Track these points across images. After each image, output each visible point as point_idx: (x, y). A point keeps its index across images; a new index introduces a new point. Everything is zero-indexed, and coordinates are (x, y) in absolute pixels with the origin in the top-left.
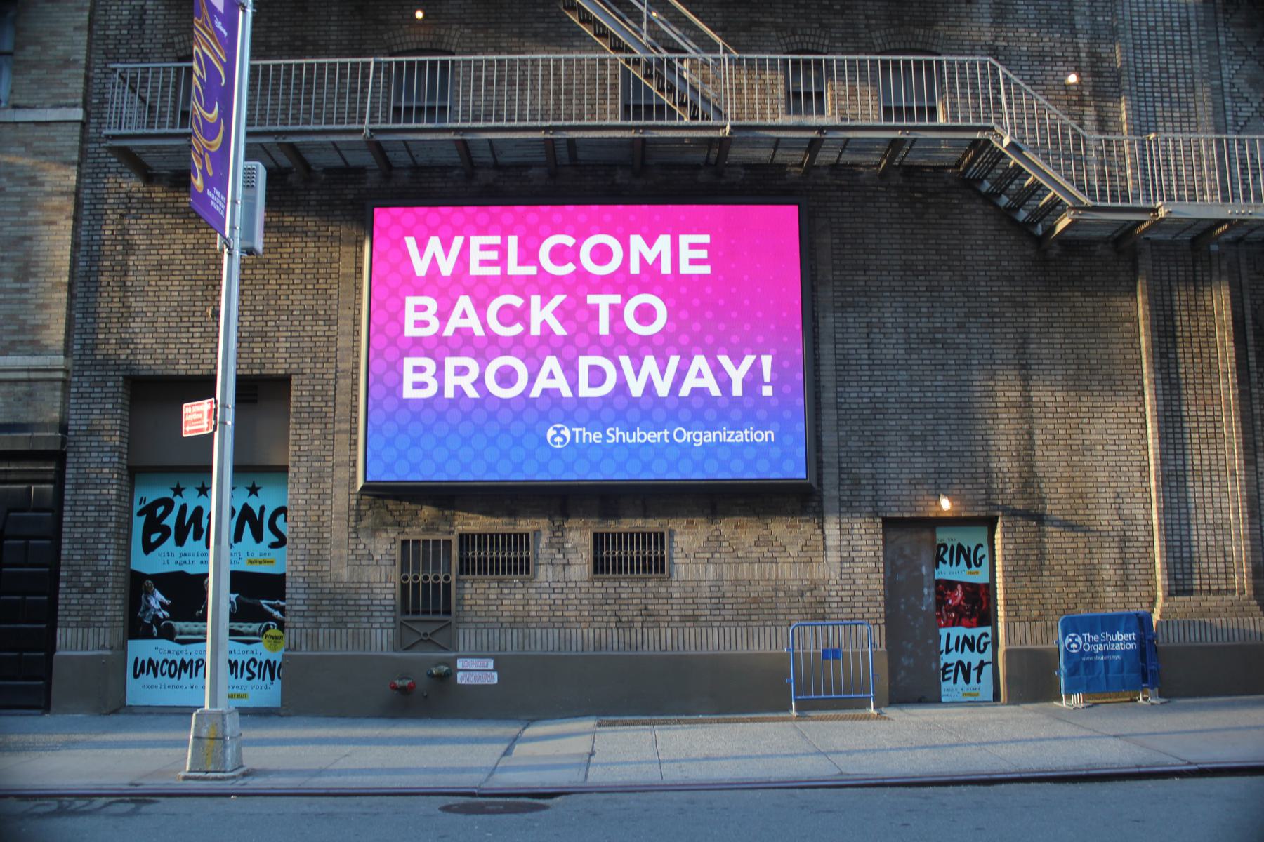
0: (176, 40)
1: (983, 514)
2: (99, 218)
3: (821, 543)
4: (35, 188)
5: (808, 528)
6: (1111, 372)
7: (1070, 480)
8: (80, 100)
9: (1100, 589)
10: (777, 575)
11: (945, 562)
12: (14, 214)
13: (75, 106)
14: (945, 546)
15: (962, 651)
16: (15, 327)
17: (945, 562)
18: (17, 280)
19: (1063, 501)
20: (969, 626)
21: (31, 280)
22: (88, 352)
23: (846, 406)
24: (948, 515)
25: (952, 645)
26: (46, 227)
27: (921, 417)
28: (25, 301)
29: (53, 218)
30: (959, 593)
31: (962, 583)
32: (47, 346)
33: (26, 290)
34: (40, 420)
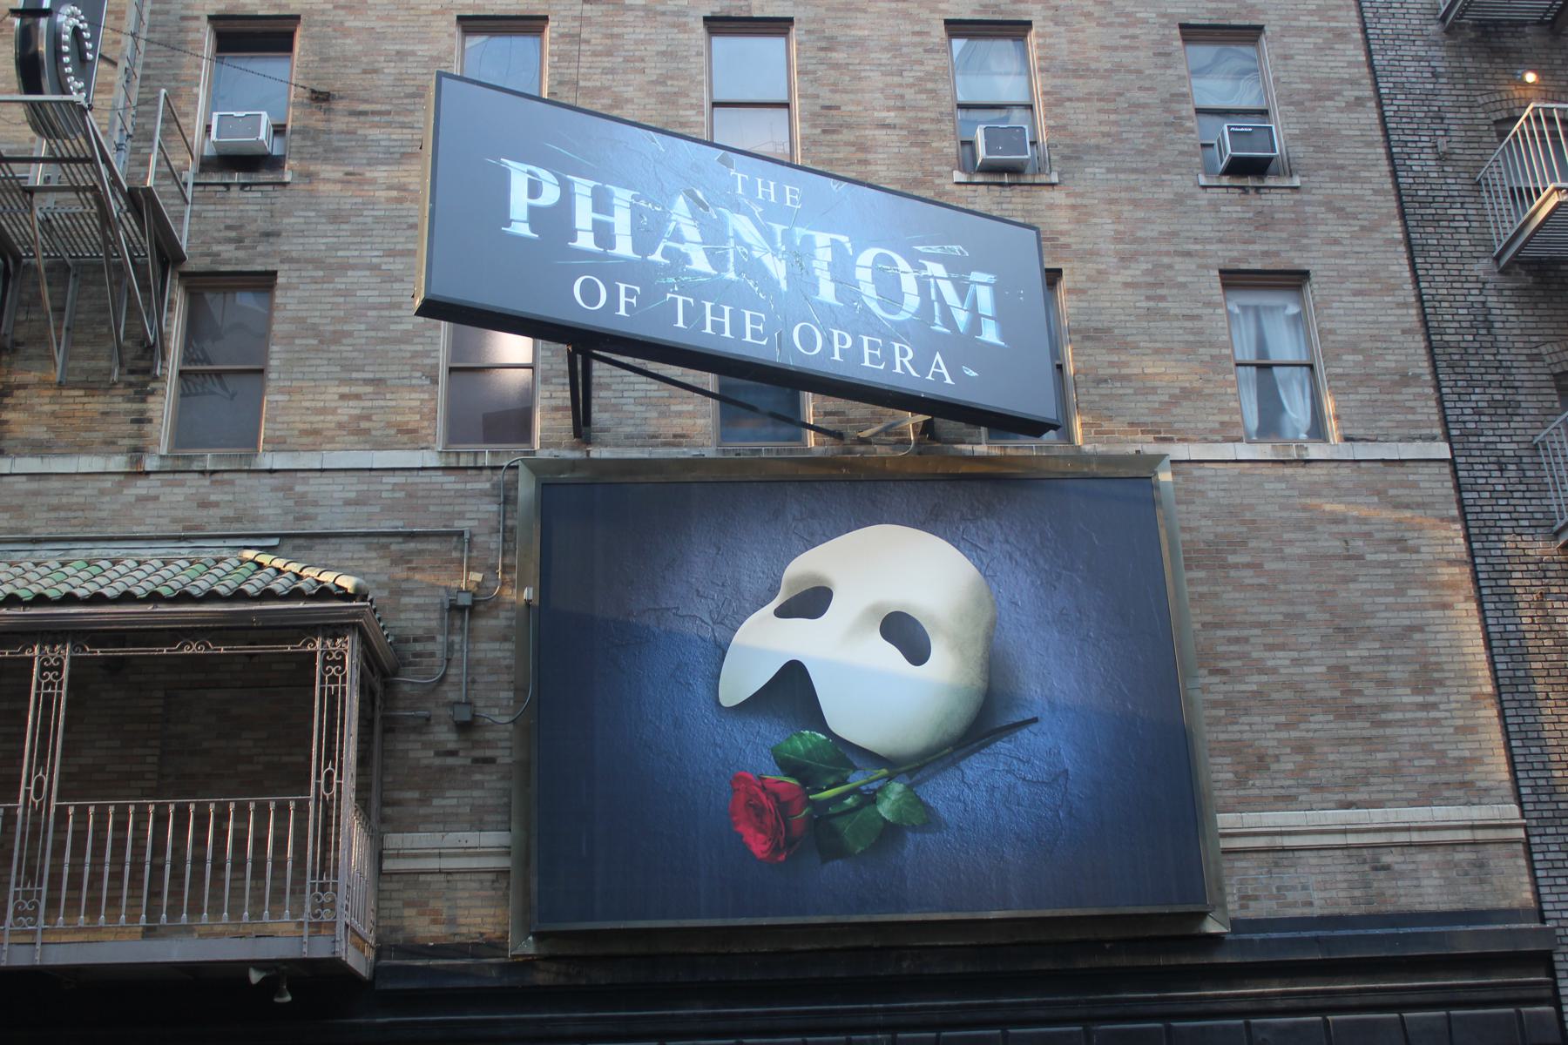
0: (1543, 350)
2: (1508, 598)
4: (1408, 556)
8: (1438, 431)
12: (1387, 593)
13: (1433, 438)
16: (1432, 762)
18: (1416, 691)
21: (1438, 690)
22: (1544, 798)
26: (1439, 613)
28: (1436, 722)
29: (1446, 599)
32: (1486, 790)
33: (1434, 706)
34: (1504, 904)
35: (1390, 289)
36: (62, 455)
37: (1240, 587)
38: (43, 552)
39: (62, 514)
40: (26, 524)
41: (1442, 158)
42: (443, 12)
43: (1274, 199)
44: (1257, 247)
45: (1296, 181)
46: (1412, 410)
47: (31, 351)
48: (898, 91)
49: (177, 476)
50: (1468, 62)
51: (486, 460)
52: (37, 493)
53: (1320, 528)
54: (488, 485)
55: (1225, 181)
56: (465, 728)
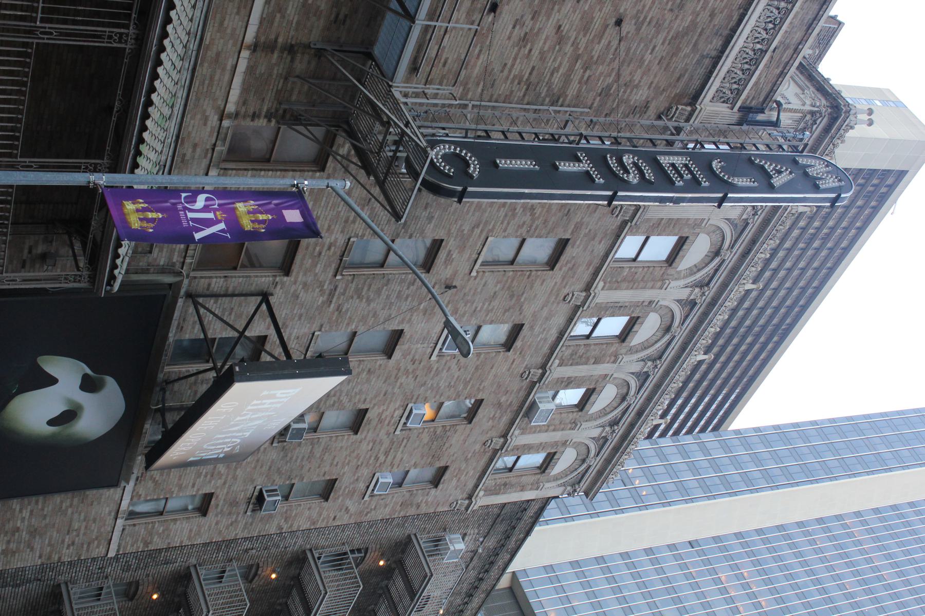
35: (189, 538)
36: (244, 80)
37: (62, 502)
38: (186, 75)
39: (207, 82)
40: (206, 65)
41: (246, 551)
42: (449, 233)
43: (243, 507)
44: (221, 503)
45: (249, 513)
46: (132, 545)
47: (313, 64)
48: (338, 394)
49: (215, 134)
50: (289, 556)
51: (188, 260)
52: (224, 70)
53: (84, 524)
54: (174, 260)
55: (256, 493)
56: (44, 257)
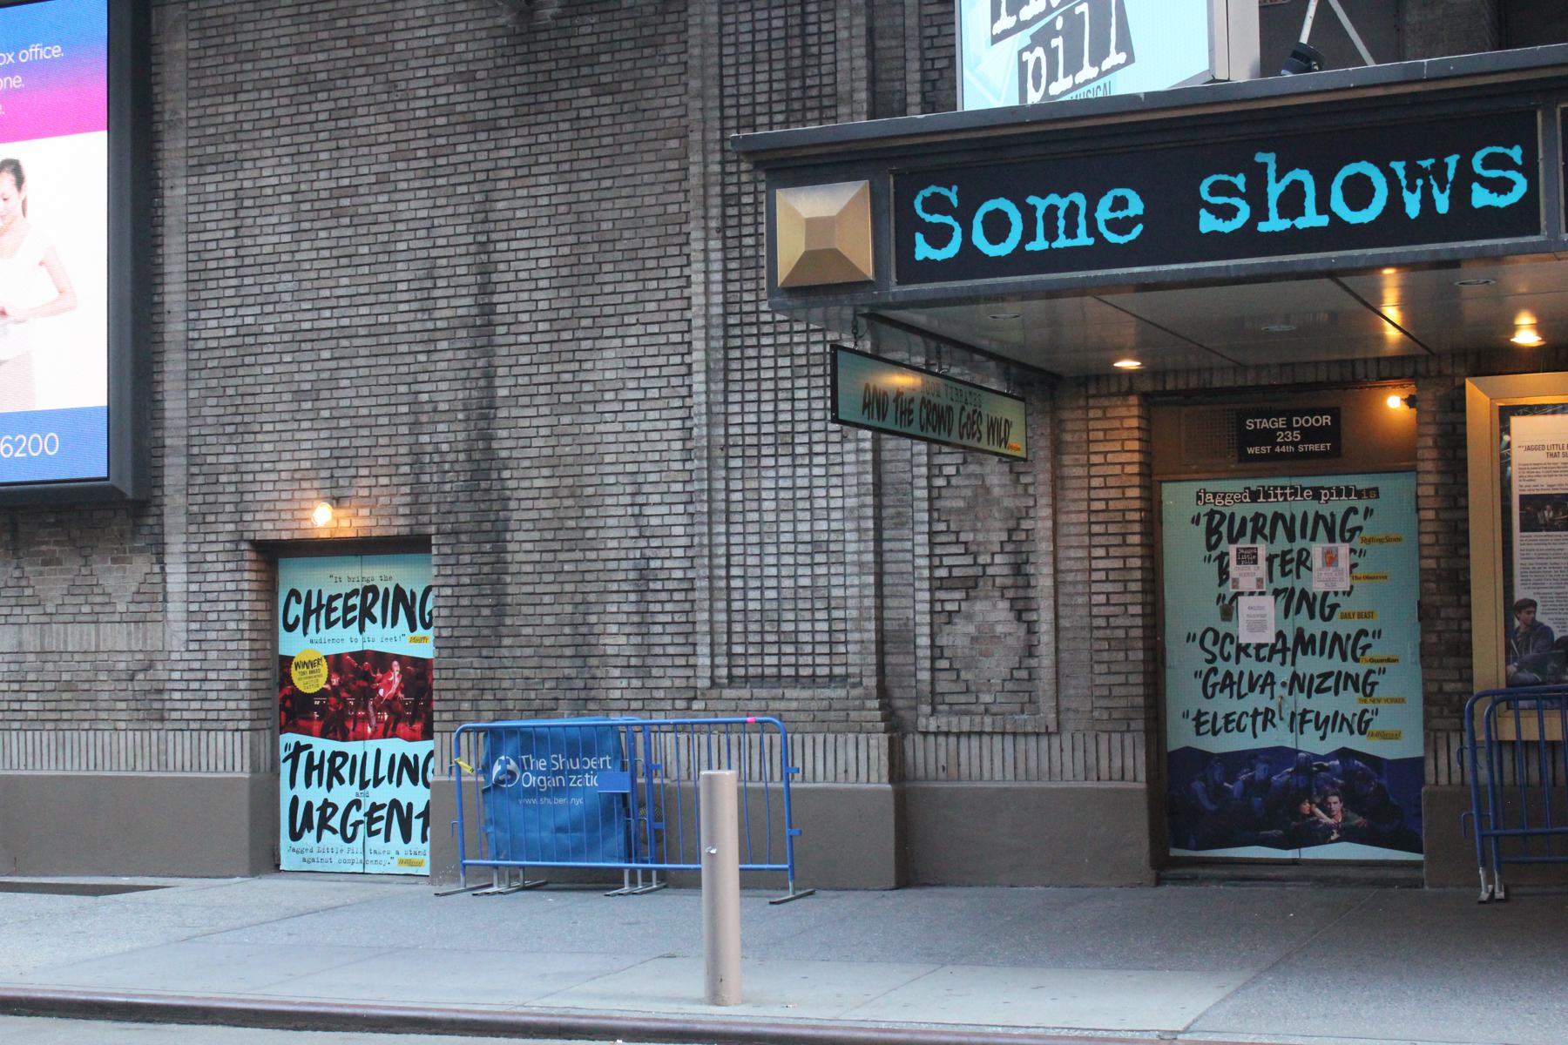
1: (405, 531)
3: (159, 588)
5: (141, 565)
6: (637, 243)
7: (554, 462)
9: (599, 673)
10: (97, 645)
11: (374, 620)
14: (374, 589)
15: (399, 783)
17: (374, 620)
19: (540, 504)
20: (411, 739)
23: (201, 345)
24: (324, 535)
25: (384, 771)
27: (313, 356)
30: (395, 677)
31: (398, 657)
